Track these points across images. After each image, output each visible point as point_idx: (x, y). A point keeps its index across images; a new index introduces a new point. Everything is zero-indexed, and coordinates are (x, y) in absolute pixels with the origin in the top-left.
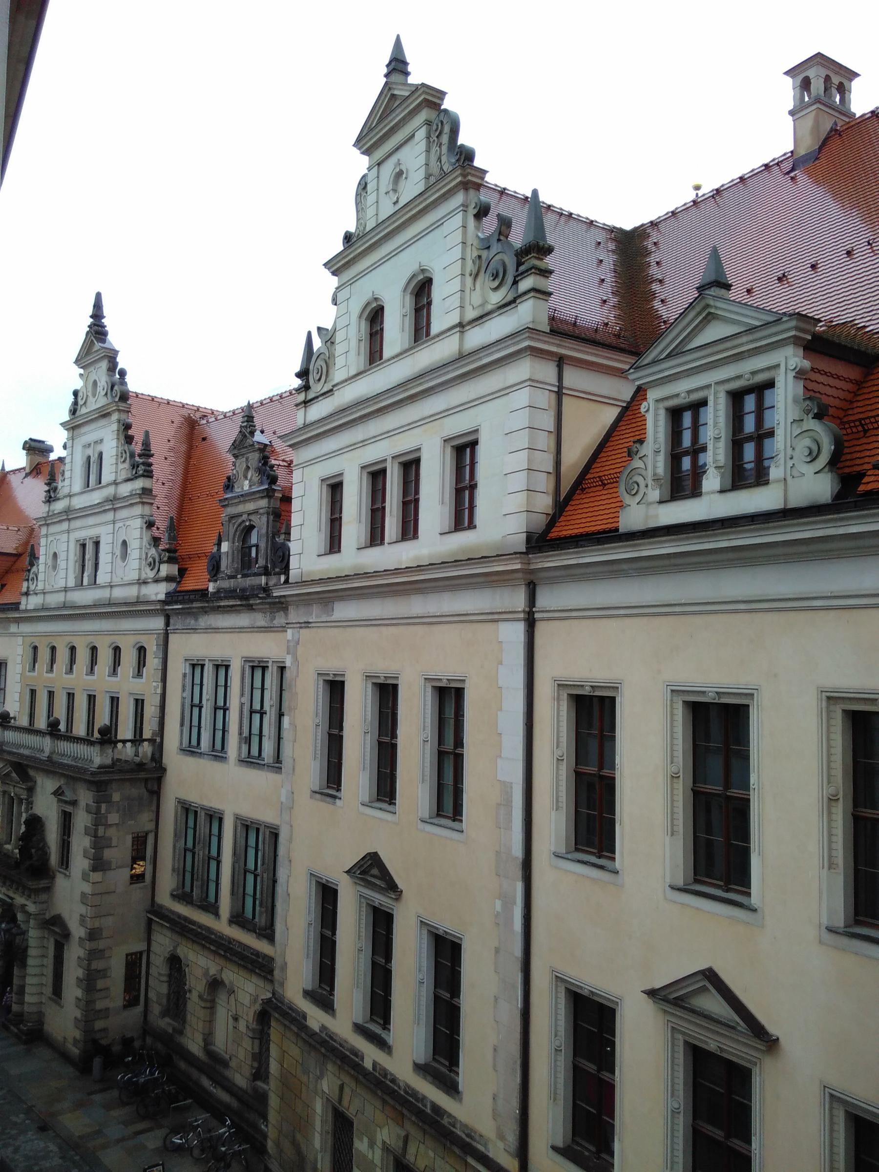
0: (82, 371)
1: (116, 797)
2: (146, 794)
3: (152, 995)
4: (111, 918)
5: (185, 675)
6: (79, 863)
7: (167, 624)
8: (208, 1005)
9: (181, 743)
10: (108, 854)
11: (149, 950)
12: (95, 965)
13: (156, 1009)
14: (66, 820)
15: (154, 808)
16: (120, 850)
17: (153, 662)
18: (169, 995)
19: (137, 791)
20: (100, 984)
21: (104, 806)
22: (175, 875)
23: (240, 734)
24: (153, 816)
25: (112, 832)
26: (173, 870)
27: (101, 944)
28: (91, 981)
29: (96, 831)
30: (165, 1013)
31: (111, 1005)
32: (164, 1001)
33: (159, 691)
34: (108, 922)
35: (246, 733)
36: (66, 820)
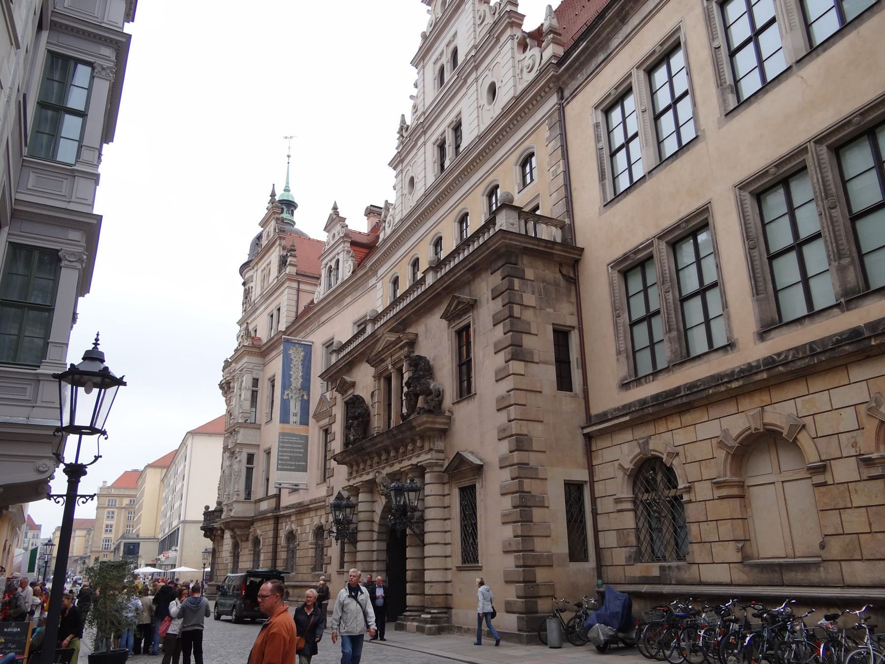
0: (429, 8)
1: (529, 274)
2: (563, 282)
3: (609, 540)
4: (540, 426)
5: (597, 126)
7: (562, 98)
8: (735, 491)
9: (605, 198)
10: (528, 341)
11: (592, 482)
12: (528, 485)
15: (573, 299)
16: (541, 343)
18: (637, 529)
19: (551, 274)
20: (537, 514)
21: (517, 282)
22: (623, 358)
23: (720, 84)
24: (573, 309)
25: (528, 315)
26: (619, 353)
27: (533, 459)
28: (525, 505)
29: (511, 310)
31: (555, 550)
32: (632, 539)
33: (561, 169)
34: (537, 431)
35: (729, 80)
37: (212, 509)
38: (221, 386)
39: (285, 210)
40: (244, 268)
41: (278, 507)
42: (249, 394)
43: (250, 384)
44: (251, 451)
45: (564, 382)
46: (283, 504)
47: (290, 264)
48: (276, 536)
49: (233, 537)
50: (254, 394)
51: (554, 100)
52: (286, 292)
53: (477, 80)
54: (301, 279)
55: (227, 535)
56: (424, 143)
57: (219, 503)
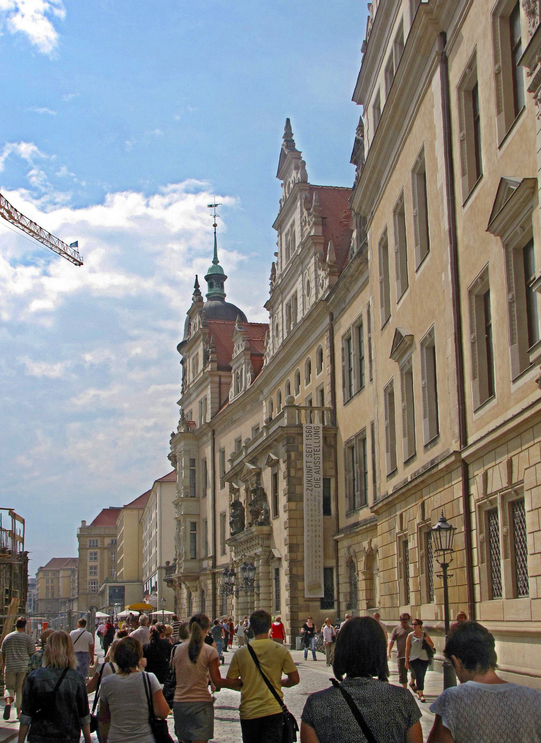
6: (283, 500)
9: (344, 401)
13: (343, 606)
14: (275, 477)
17: (326, 353)
21: (293, 454)
30: (349, 607)
36: (275, 477)
37: (171, 564)
38: (169, 458)
39: (215, 284)
40: (180, 347)
41: (214, 566)
42: (188, 472)
43: (188, 464)
44: (194, 520)
45: (327, 511)
46: (219, 563)
47: (212, 361)
48: (214, 588)
49: (188, 588)
50: (193, 472)
51: (327, 320)
52: (209, 387)
53: (302, 272)
54: (221, 373)
55: (183, 586)
56: (282, 302)
57: (175, 560)
